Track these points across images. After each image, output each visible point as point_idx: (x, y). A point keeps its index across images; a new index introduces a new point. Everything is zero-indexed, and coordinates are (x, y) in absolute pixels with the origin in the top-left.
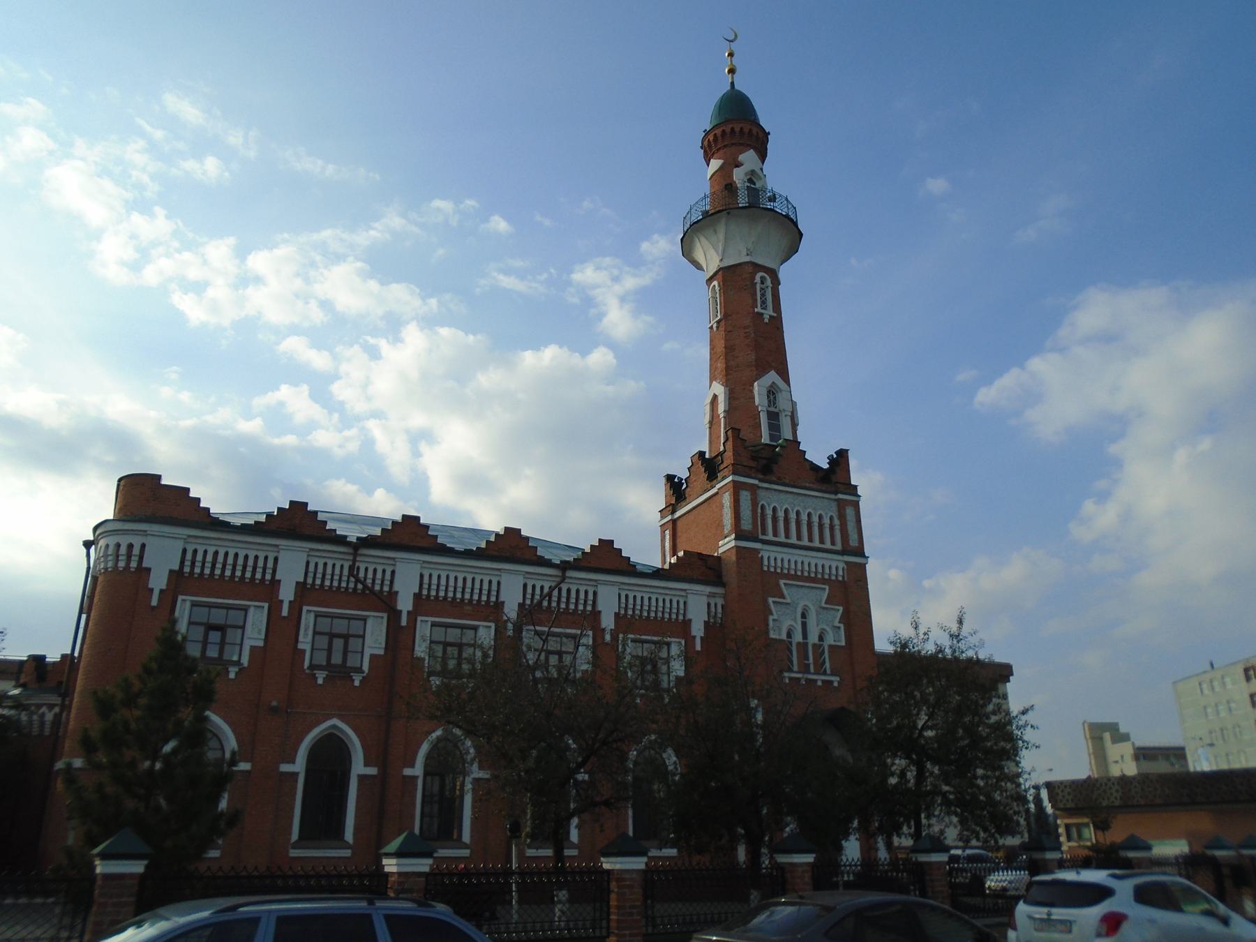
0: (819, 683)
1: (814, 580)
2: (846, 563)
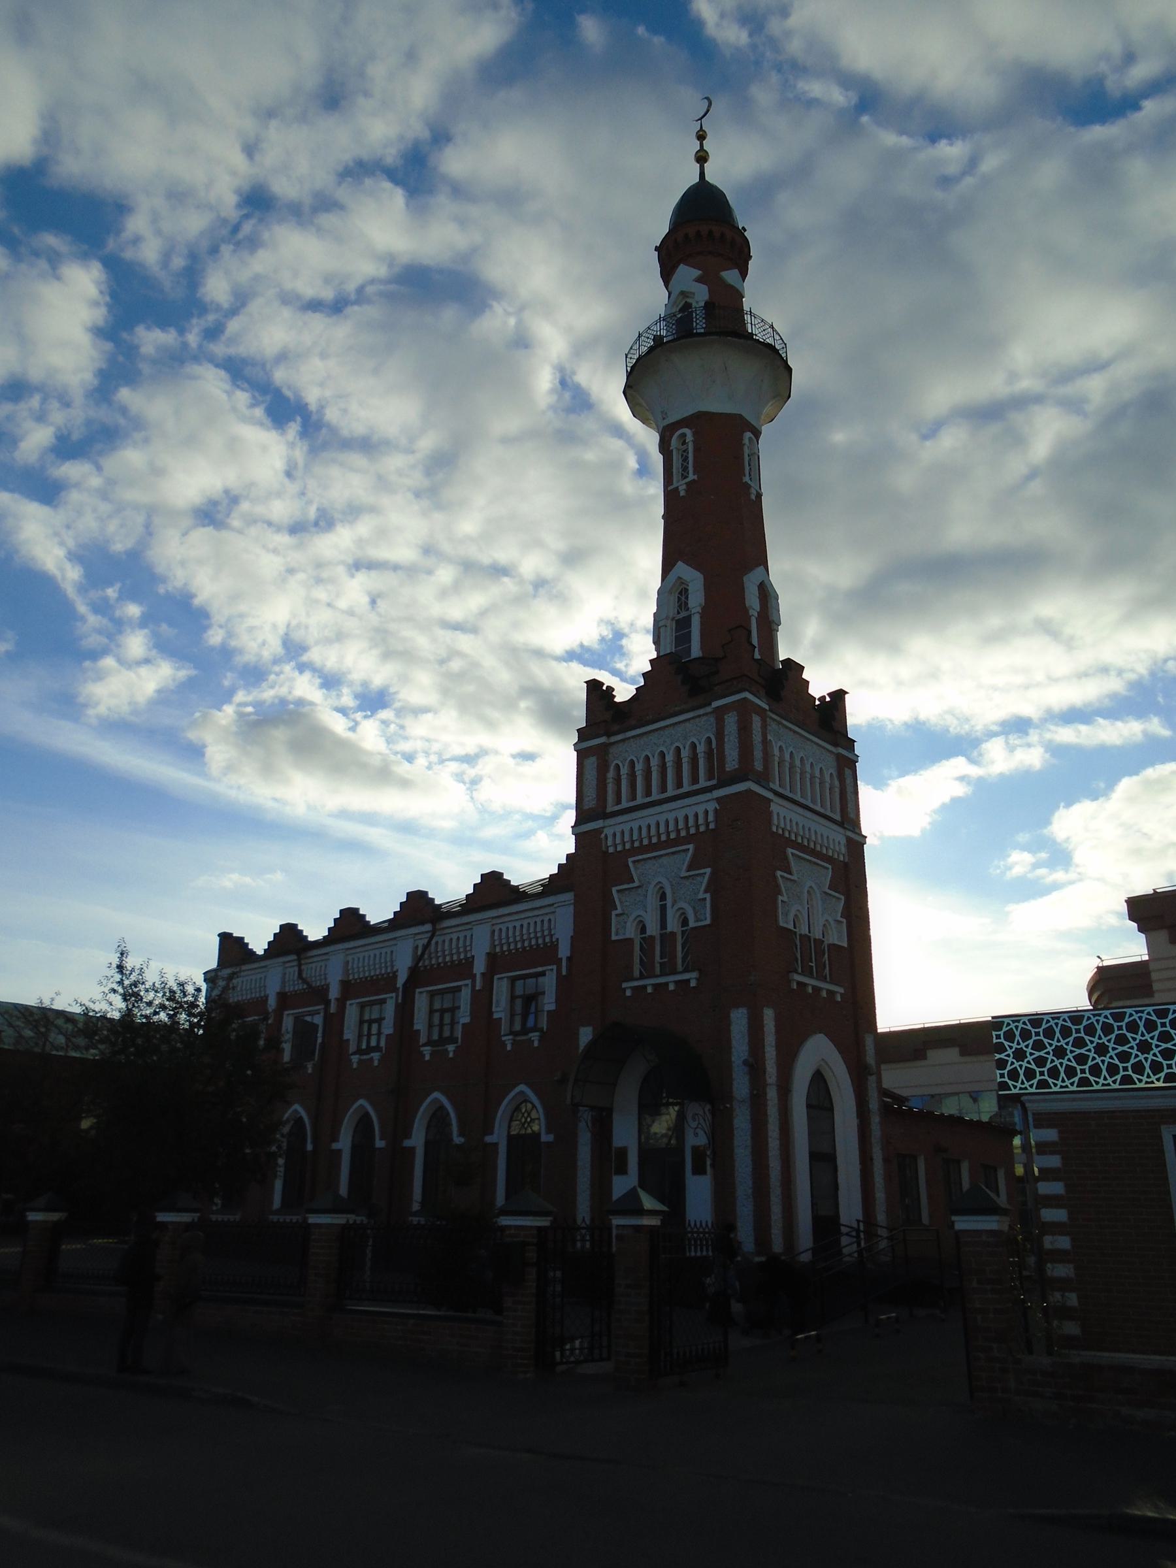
0: (672, 987)
1: (678, 841)
2: (718, 800)
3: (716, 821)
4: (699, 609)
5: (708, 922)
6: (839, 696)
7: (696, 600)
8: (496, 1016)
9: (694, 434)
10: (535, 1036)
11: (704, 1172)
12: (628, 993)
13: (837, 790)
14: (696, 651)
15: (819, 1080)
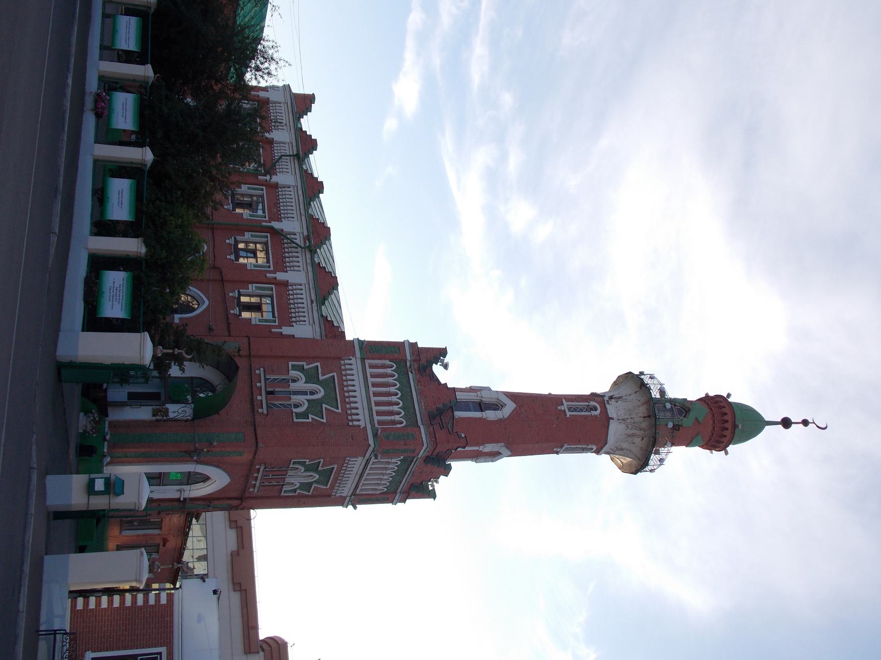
2: (365, 427)
3: (354, 426)
4: (484, 417)
5: (295, 420)
6: (432, 495)
7: (490, 415)
8: (250, 286)
9: (596, 416)
10: (236, 311)
11: (154, 415)
12: (258, 372)
13: (374, 492)
14: (458, 414)
15: (206, 479)
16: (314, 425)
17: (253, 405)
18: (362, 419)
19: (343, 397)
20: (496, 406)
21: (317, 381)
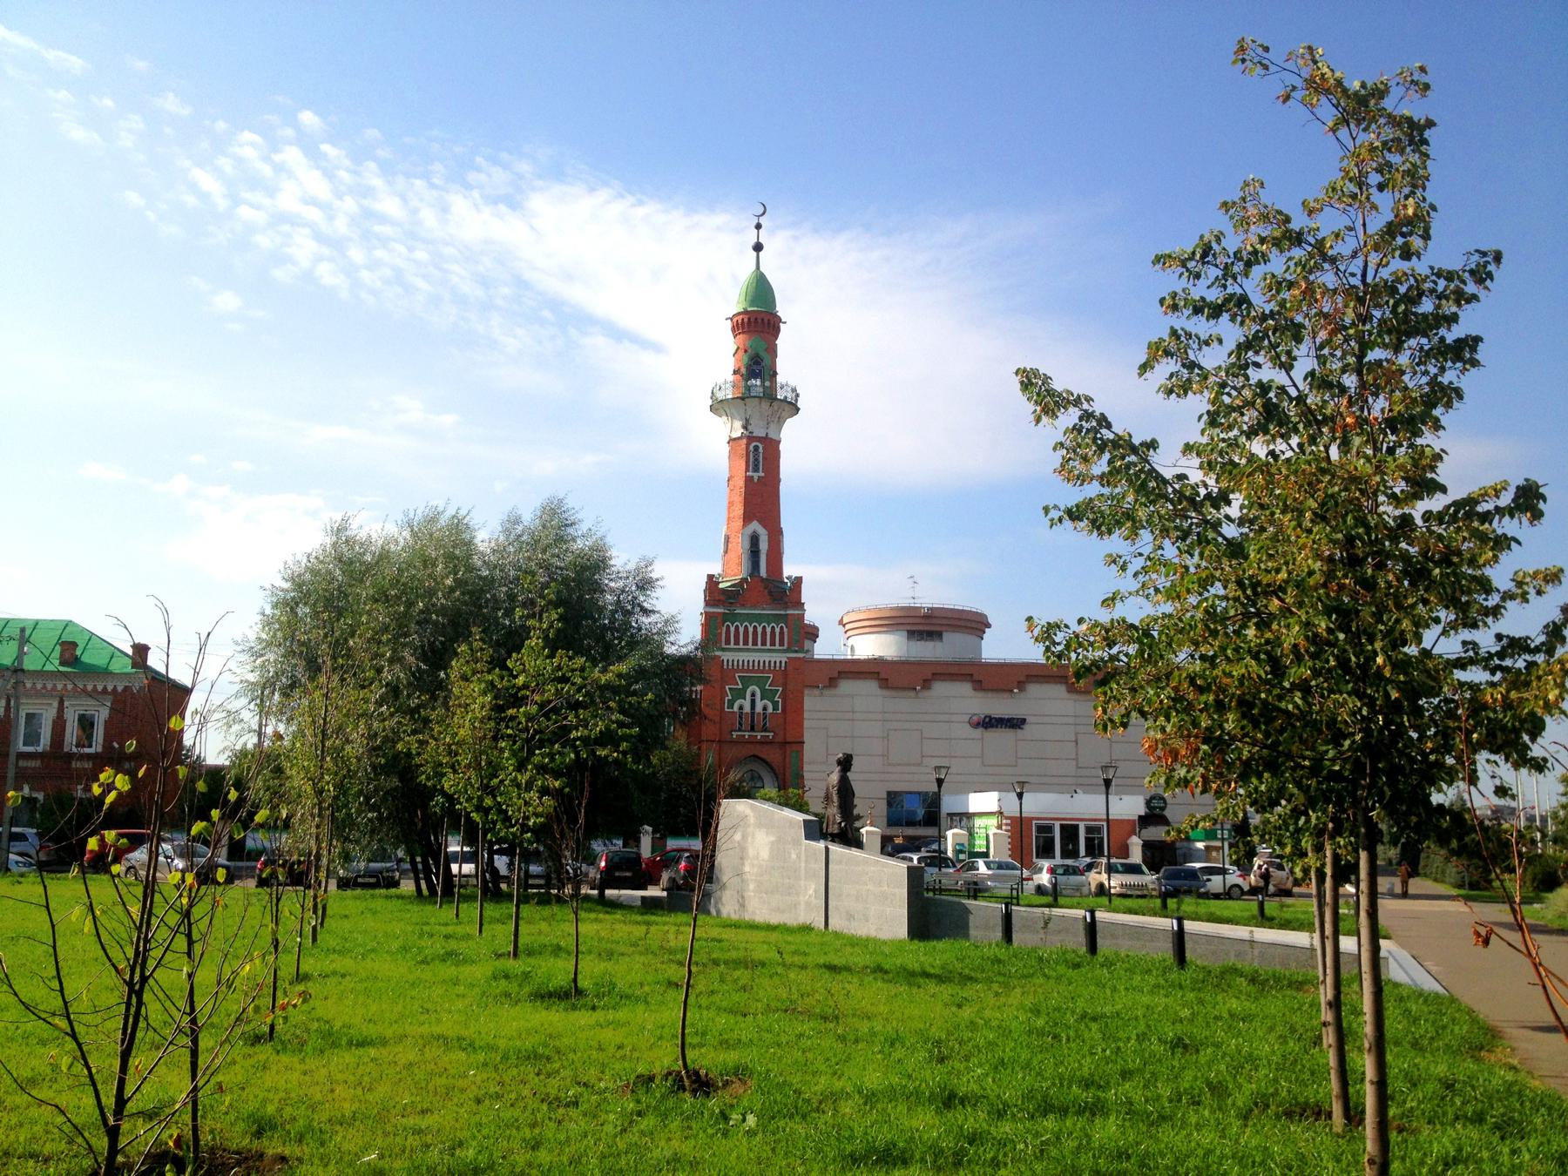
14: (763, 572)
16: (784, 697)
17: (764, 742)
18: (782, 658)
19: (758, 671)
20: (754, 540)
21: (744, 690)
